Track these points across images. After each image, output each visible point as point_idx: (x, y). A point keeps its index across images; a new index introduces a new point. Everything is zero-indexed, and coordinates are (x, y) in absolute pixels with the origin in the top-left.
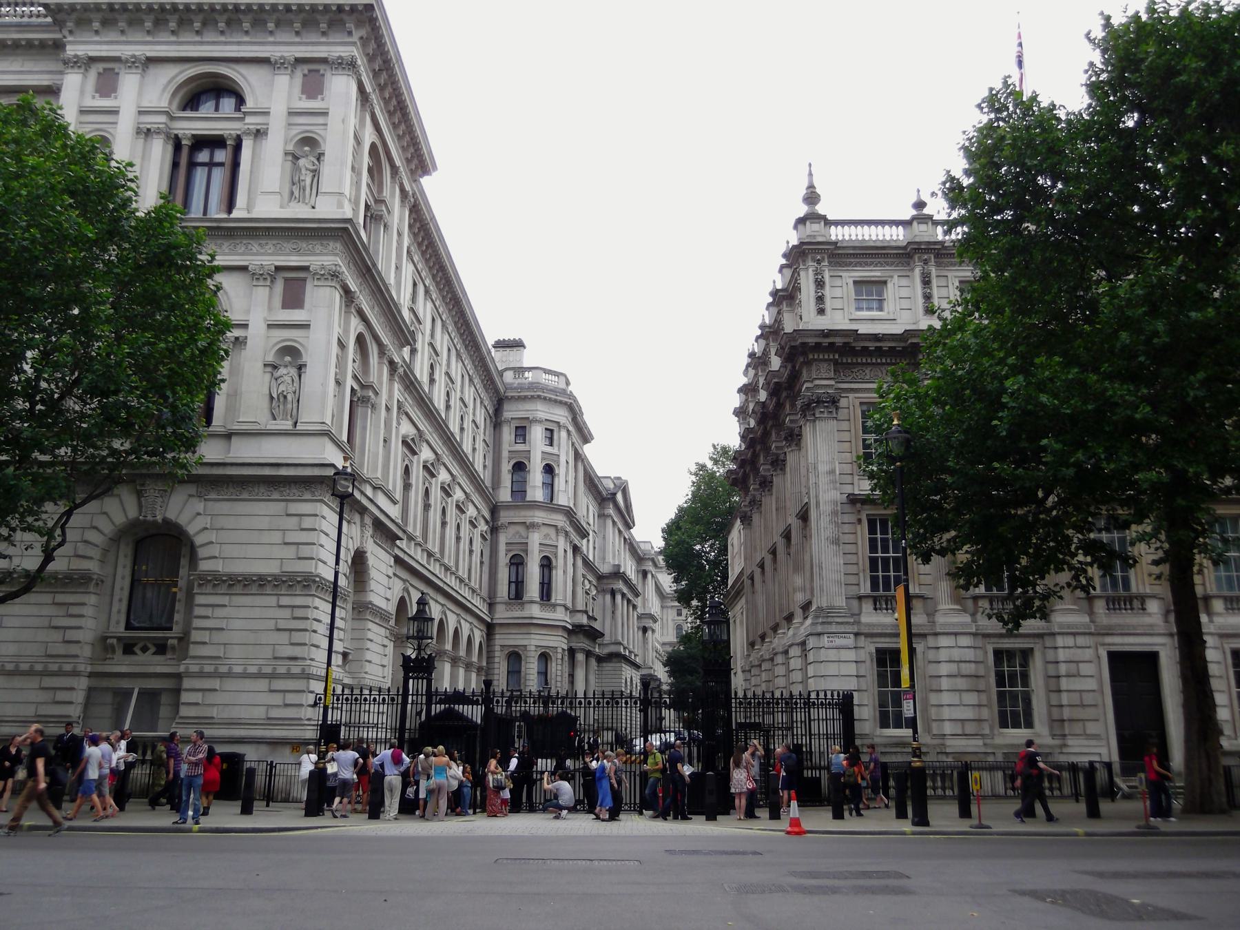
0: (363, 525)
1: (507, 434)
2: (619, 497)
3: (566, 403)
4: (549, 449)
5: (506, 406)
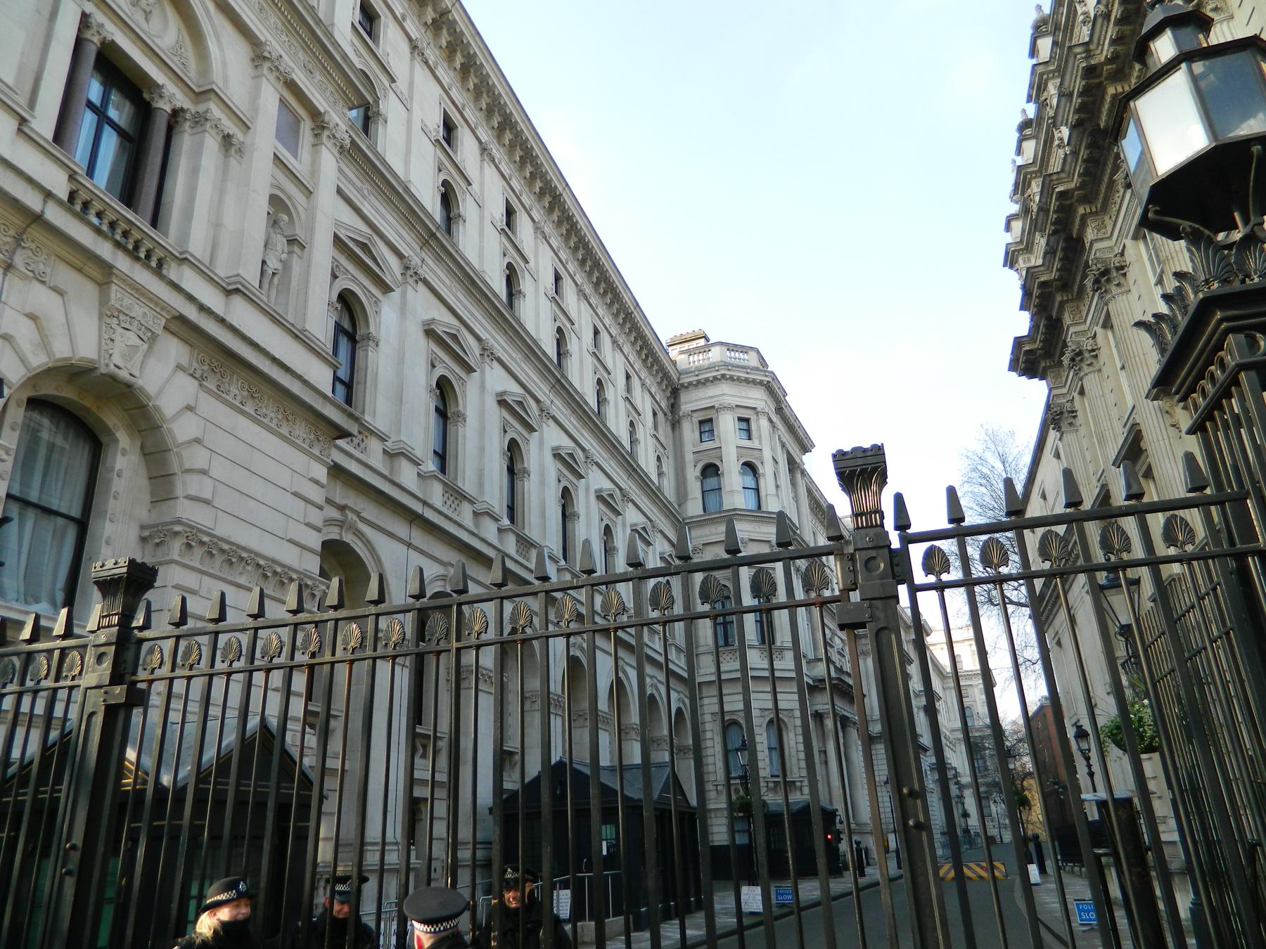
0: (107, 312)
1: (689, 431)
3: (761, 383)
4: (747, 443)
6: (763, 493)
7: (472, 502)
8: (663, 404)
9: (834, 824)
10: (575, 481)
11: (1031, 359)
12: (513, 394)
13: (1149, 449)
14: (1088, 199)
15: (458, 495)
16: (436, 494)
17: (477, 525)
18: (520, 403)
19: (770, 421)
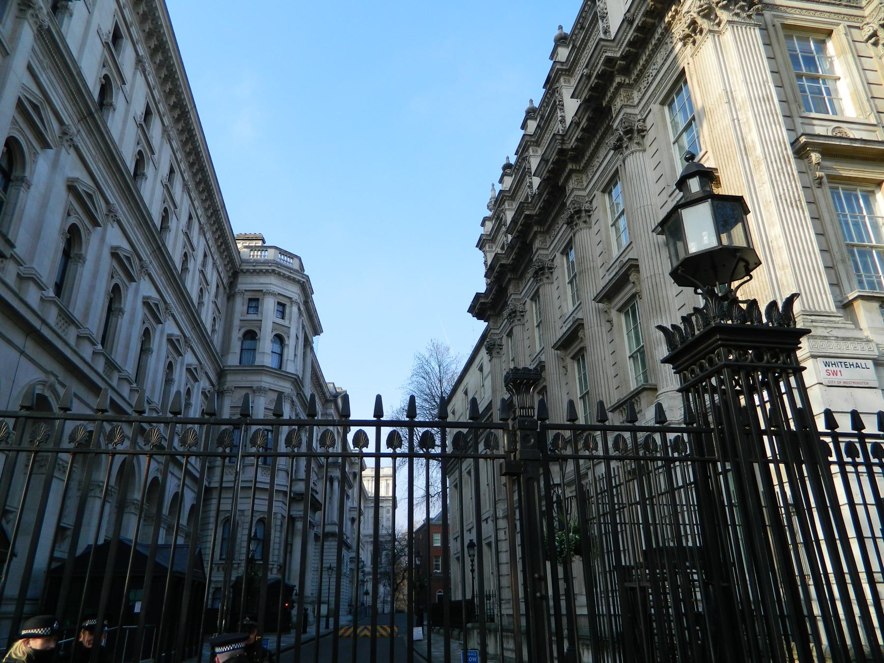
1: (240, 305)
2: (340, 401)
3: (298, 282)
4: (280, 321)
5: (241, 279)
6: (285, 357)
7: (78, 327)
8: (225, 281)
9: (291, 595)
10: (154, 324)
11: (480, 308)
12: (125, 250)
13: (547, 378)
14: (540, 223)
15: (68, 318)
16: (52, 315)
17: (77, 345)
18: (128, 258)
19: (299, 309)
